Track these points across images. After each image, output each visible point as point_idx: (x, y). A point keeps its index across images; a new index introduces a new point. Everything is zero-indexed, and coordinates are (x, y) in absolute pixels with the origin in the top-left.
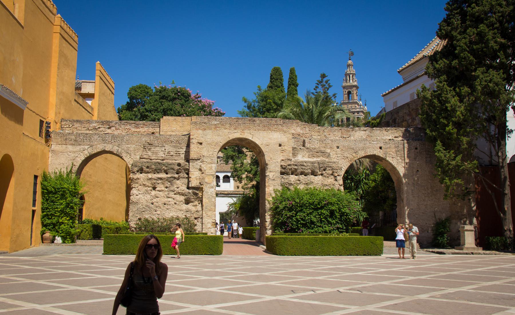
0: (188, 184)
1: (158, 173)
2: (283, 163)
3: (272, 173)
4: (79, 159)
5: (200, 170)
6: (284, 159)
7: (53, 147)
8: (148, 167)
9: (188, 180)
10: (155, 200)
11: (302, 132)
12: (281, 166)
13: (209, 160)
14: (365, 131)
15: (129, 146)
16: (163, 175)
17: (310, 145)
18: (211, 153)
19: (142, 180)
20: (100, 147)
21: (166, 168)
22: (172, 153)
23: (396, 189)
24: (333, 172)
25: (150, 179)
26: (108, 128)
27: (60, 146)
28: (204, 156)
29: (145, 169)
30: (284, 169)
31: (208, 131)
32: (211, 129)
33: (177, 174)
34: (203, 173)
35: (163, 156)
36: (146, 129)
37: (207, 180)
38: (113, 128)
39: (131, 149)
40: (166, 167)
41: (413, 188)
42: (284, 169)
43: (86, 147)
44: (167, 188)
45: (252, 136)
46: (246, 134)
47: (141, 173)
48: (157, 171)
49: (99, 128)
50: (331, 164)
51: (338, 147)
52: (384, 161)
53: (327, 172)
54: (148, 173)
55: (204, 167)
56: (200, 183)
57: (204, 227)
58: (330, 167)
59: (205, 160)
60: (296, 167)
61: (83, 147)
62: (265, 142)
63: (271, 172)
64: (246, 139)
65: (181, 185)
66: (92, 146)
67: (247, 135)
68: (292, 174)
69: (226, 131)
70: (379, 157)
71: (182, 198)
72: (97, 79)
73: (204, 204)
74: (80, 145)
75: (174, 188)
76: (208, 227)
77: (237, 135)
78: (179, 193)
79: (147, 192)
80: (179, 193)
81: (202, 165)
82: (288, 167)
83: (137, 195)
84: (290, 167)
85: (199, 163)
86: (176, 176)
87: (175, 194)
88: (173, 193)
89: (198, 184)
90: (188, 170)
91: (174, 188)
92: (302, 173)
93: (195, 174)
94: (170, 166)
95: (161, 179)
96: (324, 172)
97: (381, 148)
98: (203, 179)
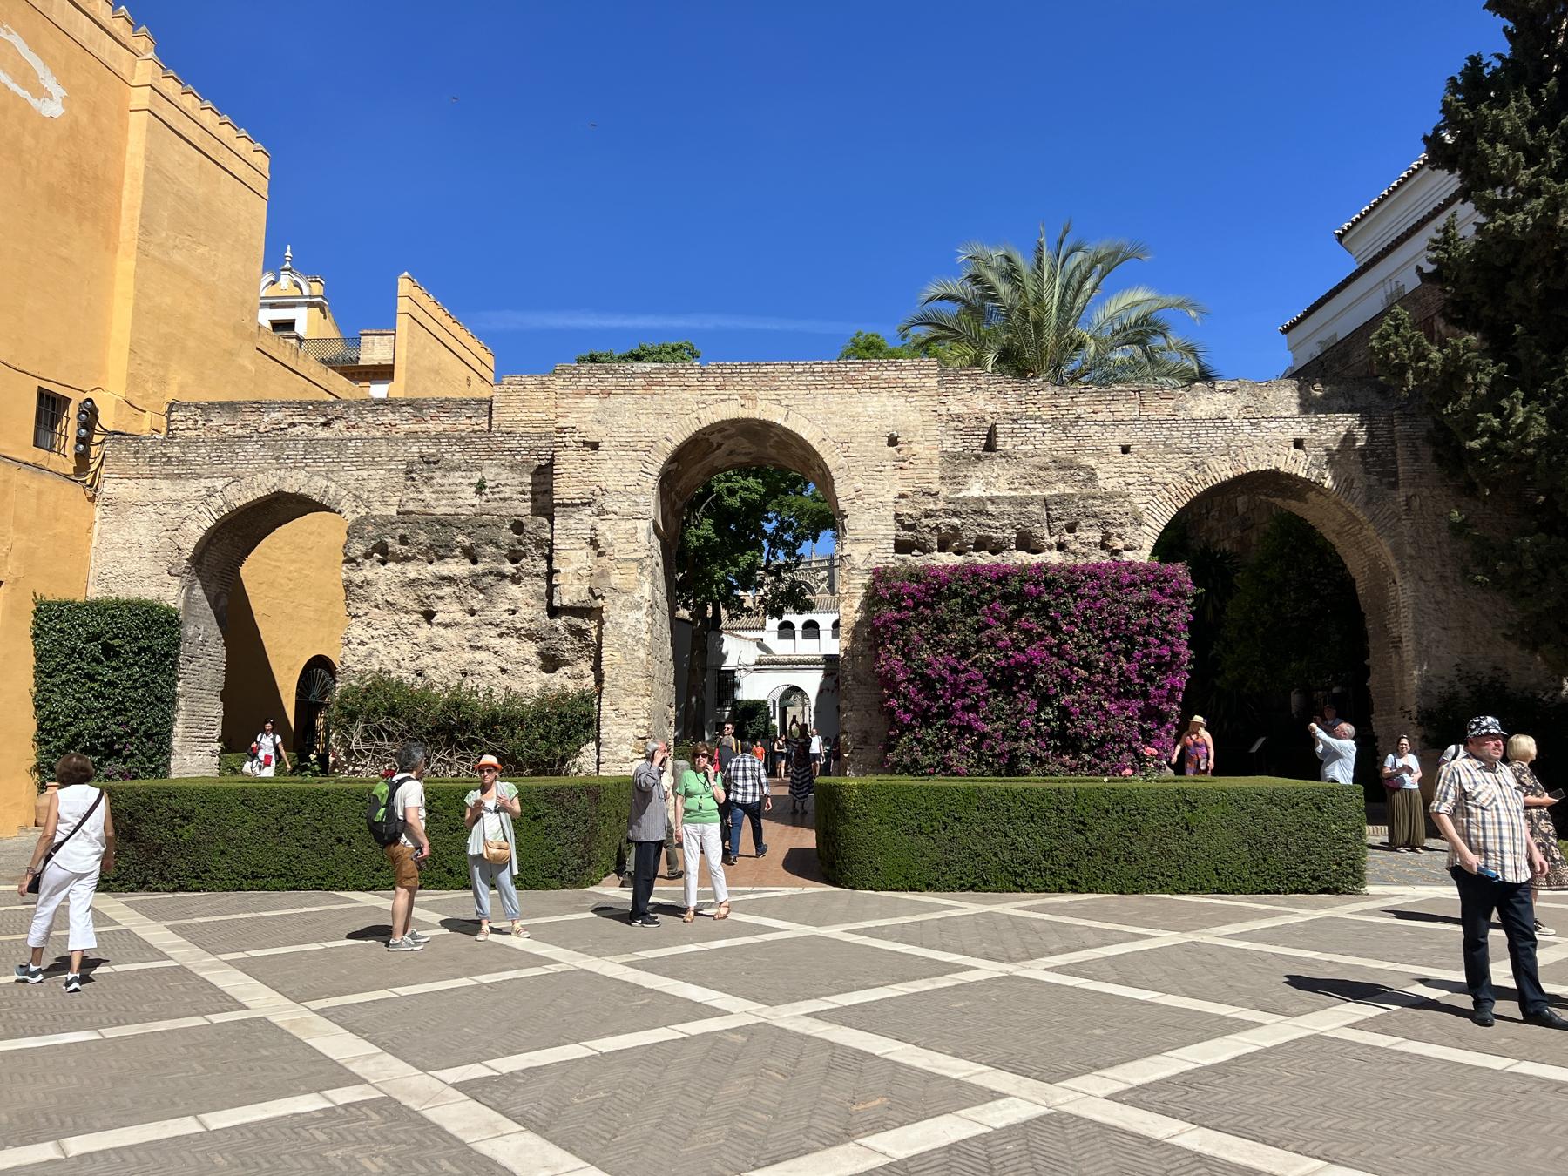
0: (550, 595)
1: (441, 558)
2: (905, 508)
3: (864, 548)
4: (193, 526)
5: (593, 543)
6: (907, 490)
7: (107, 488)
9: (549, 581)
10: (427, 660)
11: (991, 407)
12: (897, 515)
13: (625, 506)
14: (1232, 390)
15: (365, 473)
16: (458, 567)
17: (1018, 441)
18: (632, 479)
19: (383, 588)
20: (261, 485)
21: (467, 543)
22: (507, 492)
23: (1365, 603)
24: (1107, 536)
25: (413, 583)
26: (324, 425)
27: (131, 483)
28: (604, 491)
29: (394, 546)
30: (911, 527)
31: (621, 399)
32: (626, 391)
33: (514, 561)
34: (600, 554)
35: (476, 501)
37: (615, 579)
38: (339, 425)
39: (373, 485)
40: (469, 535)
41: (1440, 594)
42: (911, 527)
43: (219, 484)
44: (472, 613)
45: (784, 411)
46: (762, 405)
47: (383, 563)
48: (438, 552)
49: (293, 425)
50: (1097, 506)
51: (1125, 450)
52: (1312, 495)
53: (1083, 535)
54: (407, 559)
55: (608, 531)
56: (591, 591)
57: (604, 756)
58: (1095, 516)
59: (609, 506)
60: (956, 521)
61: (208, 483)
62: (833, 432)
64: (767, 426)
65: (522, 600)
66: (237, 479)
67: (767, 409)
68: (942, 549)
69: (686, 395)
70: (1296, 478)
71: (530, 649)
72: (402, 322)
73: (605, 668)
74: (199, 477)
75: (500, 611)
76: (622, 755)
77: (728, 408)
79: (399, 631)
80: (517, 630)
81: (599, 526)
82: (925, 521)
83: (362, 643)
84: (932, 522)
86: (509, 568)
87: (501, 635)
88: (494, 632)
89: (585, 595)
90: (551, 544)
91: (500, 611)
92: (981, 544)
93: (574, 561)
94: (485, 533)
95: (450, 580)
96: (1069, 537)
97: (1298, 444)
98: (604, 575)
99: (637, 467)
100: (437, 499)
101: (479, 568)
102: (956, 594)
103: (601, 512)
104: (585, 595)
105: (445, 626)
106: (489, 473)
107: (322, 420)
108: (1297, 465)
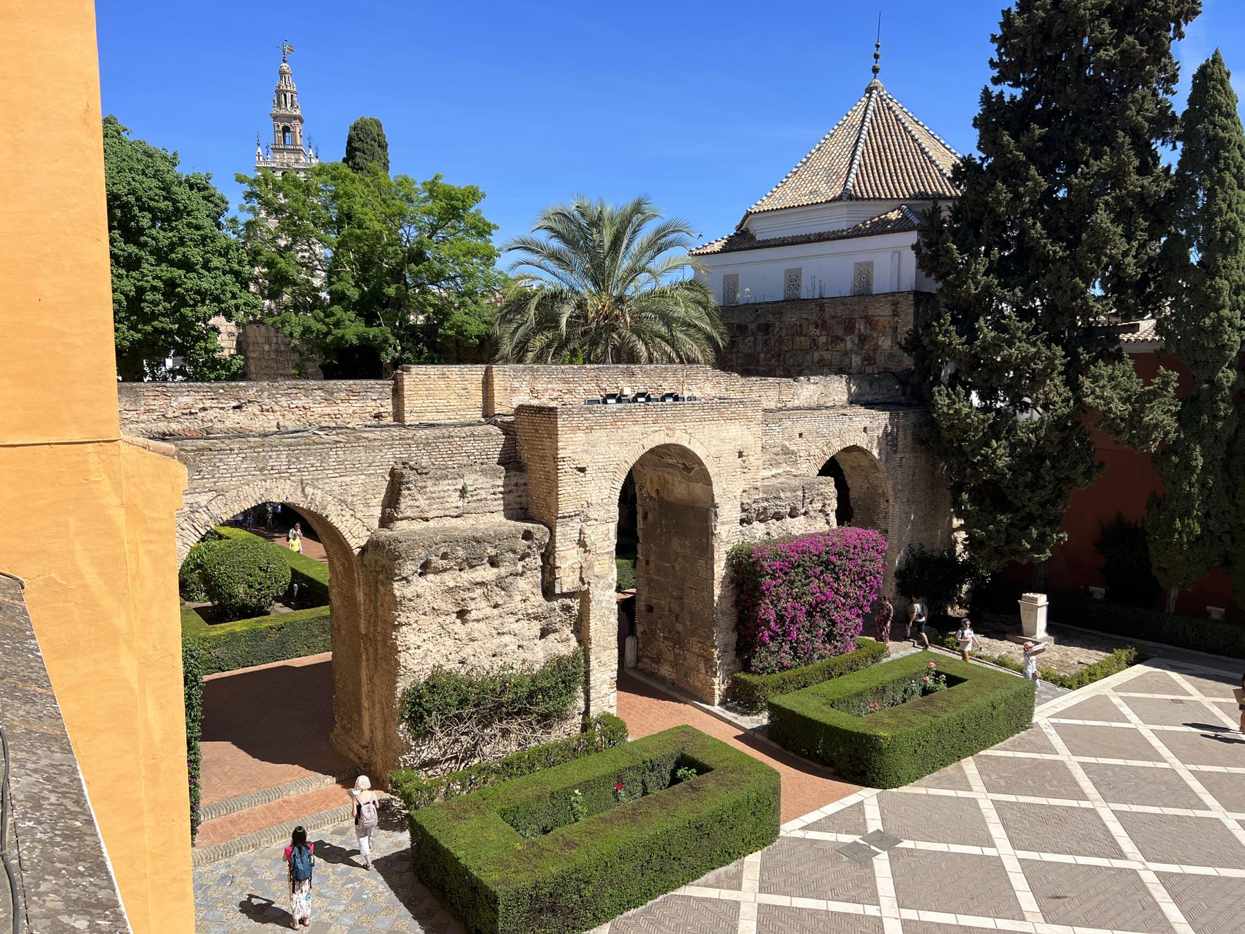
1: (472, 567)
3: (726, 527)
5: (582, 543)
8: (444, 556)
10: (468, 651)
15: (347, 479)
16: (486, 573)
18: (607, 492)
22: (483, 494)
36: (356, 405)
37: (597, 570)
39: (355, 489)
43: (203, 499)
45: (688, 437)
49: (204, 409)
51: (801, 435)
54: (445, 570)
56: (582, 579)
57: (593, 695)
59: (593, 514)
63: (723, 523)
66: (220, 493)
67: (680, 438)
69: (636, 428)
71: (536, 627)
75: (516, 603)
77: (659, 438)
78: (529, 617)
83: (419, 647)
85: (576, 524)
88: (512, 619)
98: (591, 567)
99: (609, 484)
100: (429, 505)
101: (503, 571)
102: (799, 566)
103: (587, 519)
104: (577, 583)
105: (478, 621)
106: (470, 480)
107: (235, 404)
108: (862, 441)
